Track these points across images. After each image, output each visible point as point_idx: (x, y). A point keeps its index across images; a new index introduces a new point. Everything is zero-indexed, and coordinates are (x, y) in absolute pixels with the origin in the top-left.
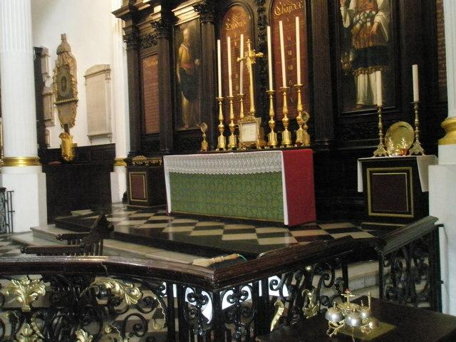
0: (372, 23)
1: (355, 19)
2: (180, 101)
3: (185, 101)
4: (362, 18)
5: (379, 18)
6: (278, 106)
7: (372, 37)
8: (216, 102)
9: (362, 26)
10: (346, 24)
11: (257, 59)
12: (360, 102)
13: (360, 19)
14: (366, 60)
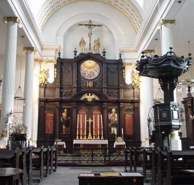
2: (62, 127)
3: (64, 127)
5: (116, 119)
6: (96, 131)
7: (115, 122)
8: (77, 128)
9: (113, 120)
10: (110, 119)
12: (112, 133)
14: (114, 125)
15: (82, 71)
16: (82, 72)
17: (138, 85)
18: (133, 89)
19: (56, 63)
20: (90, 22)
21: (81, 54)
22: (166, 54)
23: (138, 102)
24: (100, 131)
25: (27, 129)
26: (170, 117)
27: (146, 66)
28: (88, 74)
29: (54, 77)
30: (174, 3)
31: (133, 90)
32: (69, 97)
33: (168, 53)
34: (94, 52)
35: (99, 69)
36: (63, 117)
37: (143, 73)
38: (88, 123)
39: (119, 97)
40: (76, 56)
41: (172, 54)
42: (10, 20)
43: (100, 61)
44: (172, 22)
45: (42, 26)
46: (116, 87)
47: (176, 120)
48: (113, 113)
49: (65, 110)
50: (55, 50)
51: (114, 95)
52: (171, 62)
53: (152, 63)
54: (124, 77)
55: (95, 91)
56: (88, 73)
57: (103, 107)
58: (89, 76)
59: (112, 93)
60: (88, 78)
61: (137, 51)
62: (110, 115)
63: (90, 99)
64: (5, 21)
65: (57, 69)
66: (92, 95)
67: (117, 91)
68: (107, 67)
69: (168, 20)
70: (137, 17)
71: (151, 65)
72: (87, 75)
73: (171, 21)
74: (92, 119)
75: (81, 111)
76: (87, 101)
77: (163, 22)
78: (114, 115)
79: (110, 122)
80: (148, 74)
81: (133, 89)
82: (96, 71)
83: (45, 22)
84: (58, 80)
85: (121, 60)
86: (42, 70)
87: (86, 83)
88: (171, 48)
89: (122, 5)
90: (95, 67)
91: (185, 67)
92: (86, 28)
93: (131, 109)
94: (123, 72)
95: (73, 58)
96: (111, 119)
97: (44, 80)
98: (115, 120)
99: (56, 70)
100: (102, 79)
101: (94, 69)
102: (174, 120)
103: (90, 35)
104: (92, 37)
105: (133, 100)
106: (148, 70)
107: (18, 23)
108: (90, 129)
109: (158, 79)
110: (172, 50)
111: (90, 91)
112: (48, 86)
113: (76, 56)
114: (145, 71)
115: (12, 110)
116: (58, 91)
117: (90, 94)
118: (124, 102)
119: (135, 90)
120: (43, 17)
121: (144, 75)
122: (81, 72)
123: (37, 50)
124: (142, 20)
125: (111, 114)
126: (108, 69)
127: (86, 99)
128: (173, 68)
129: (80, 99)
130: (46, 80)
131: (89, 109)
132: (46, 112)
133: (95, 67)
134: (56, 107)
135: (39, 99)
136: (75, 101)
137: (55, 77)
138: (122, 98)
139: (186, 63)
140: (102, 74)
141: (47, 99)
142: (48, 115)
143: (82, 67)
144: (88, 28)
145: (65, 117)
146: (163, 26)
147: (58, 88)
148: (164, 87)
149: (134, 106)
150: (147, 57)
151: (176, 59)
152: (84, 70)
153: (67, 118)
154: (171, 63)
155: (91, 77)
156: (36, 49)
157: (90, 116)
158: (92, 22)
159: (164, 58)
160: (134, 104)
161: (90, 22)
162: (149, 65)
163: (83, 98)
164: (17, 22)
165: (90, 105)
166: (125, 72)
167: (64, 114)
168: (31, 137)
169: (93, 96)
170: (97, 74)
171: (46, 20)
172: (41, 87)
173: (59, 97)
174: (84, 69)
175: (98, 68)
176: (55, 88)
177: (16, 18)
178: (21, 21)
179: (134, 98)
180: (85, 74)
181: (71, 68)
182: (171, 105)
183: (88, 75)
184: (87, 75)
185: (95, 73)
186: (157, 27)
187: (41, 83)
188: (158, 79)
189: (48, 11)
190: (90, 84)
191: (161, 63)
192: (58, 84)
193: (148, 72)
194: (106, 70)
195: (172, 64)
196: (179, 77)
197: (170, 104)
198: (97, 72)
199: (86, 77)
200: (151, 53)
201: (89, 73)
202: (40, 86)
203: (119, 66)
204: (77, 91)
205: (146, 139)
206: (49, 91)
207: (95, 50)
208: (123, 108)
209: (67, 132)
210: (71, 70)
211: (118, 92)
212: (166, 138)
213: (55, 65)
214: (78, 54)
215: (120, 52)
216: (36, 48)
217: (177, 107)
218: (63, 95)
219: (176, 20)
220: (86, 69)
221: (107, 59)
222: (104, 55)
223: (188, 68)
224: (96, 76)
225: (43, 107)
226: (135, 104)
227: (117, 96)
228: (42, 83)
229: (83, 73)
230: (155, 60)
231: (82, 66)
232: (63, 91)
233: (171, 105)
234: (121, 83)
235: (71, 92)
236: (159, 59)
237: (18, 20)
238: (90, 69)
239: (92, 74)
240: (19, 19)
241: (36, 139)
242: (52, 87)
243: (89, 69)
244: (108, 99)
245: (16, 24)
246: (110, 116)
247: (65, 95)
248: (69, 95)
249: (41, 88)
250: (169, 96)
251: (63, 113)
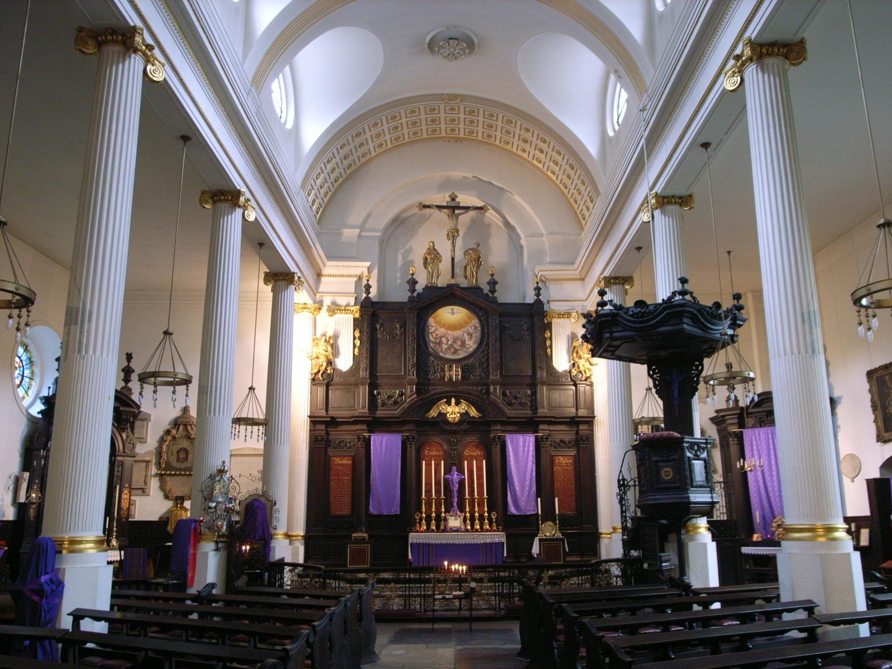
16: (432, 339)
17: (588, 375)
18: (575, 385)
19: (357, 315)
20: (453, 200)
21: (426, 288)
22: (670, 299)
23: (590, 421)
24: (481, 505)
25: (274, 508)
26: (684, 481)
27: (611, 333)
28: (447, 344)
29: (354, 354)
30: (689, 149)
31: (574, 388)
33: (674, 294)
34: (464, 283)
37: (604, 352)
39: (536, 409)
40: (415, 294)
41: (688, 297)
42: (220, 200)
43: (481, 309)
44: (684, 201)
45: (317, 212)
46: (528, 381)
47: (701, 486)
50: (355, 279)
51: (521, 404)
52: (685, 320)
53: (630, 324)
54: (549, 350)
55: (470, 394)
56: (448, 340)
57: (492, 436)
58: (452, 350)
59: (516, 398)
60: (447, 356)
61: (583, 279)
63: (453, 416)
64: (207, 202)
67: (529, 392)
68: (500, 322)
69: (673, 196)
70: (583, 183)
71: (629, 330)
72: (444, 346)
73: (680, 198)
75: (429, 450)
77: (657, 201)
80: (617, 353)
81: (575, 385)
82: (470, 335)
83: (326, 200)
84: (365, 363)
85: (539, 303)
86: (318, 335)
87: (443, 370)
88: (683, 281)
89: (542, 151)
90: (466, 323)
91: (726, 334)
92: (443, 215)
93: (570, 442)
94: (545, 339)
95: (406, 300)
97: (325, 364)
99: (357, 334)
100: (488, 358)
101: (465, 329)
102: (696, 487)
103: (453, 235)
104: (459, 242)
106: (618, 343)
107: (245, 208)
108: (454, 498)
109: (645, 367)
110: (686, 285)
111: (455, 394)
112: (336, 379)
113: (415, 294)
114: (609, 346)
115: (224, 462)
116: (363, 392)
117: (453, 400)
118: (550, 423)
119: (581, 388)
120: (321, 187)
121: (604, 354)
123: (302, 279)
124: (598, 193)
126: (502, 329)
127: (442, 415)
128: (692, 337)
130: (330, 363)
131: (450, 443)
132: (331, 452)
133: (466, 323)
134: (359, 439)
135: (310, 417)
136: (409, 422)
137: (356, 354)
138: (542, 412)
139: (728, 322)
141: (332, 418)
142: (338, 460)
144: (446, 217)
146: (657, 213)
147: (363, 384)
148: (663, 389)
149: (577, 433)
150: (615, 306)
151: (699, 311)
154: (683, 323)
155: (456, 352)
156: (299, 278)
157: (454, 462)
158: (457, 200)
159: (665, 309)
161: (453, 200)
162: (620, 329)
163: (433, 413)
164: (239, 207)
165: (455, 432)
168: (288, 529)
169: (464, 407)
170: (474, 342)
171: (330, 194)
172: (316, 382)
173: (366, 410)
175: (476, 328)
176: (356, 385)
177: (238, 193)
178: (253, 202)
179: (577, 410)
180: (440, 343)
181: (401, 327)
182: (685, 445)
183: (449, 348)
184: (444, 346)
185: (467, 342)
186: (641, 214)
187: (316, 371)
188: (645, 367)
189: (334, 169)
190: (455, 373)
191: (654, 324)
192: (364, 374)
193: (617, 347)
195: (687, 327)
196: (706, 361)
197: (683, 442)
199: (441, 354)
200: (623, 284)
201: (450, 343)
202: (313, 380)
203: (534, 319)
204: (418, 392)
205: (614, 529)
206: (337, 392)
207: (466, 277)
208: (547, 438)
210: (401, 334)
211: (534, 394)
212: (673, 537)
213: (355, 319)
214: (419, 288)
215: (537, 283)
216: (299, 274)
217: (704, 450)
218: (380, 405)
219: (695, 197)
220: (442, 331)
221: (499, 301)
222: (493, 291)
223: (732, 336)
224: (471, 349)
225: (322, 439)
226: (582, 427)
227: (529, 404)
228: (319, 371)
230: (637, 314)
231: (431, 321)
232: (379, 393)
233: (685, 445)
234: (540, 368)
235: (401, 395)
236: (650, 313)
237: (242, 199)
238: (453, 327)
239: (459, 343)
240: (248, 195)
241: (300, 530)
242: (349, 380)
244: (503, 413)
245: (239, 212)
247: (383, 404)
248: (396, 403)
249: (315, 385)
250: (678, 413)
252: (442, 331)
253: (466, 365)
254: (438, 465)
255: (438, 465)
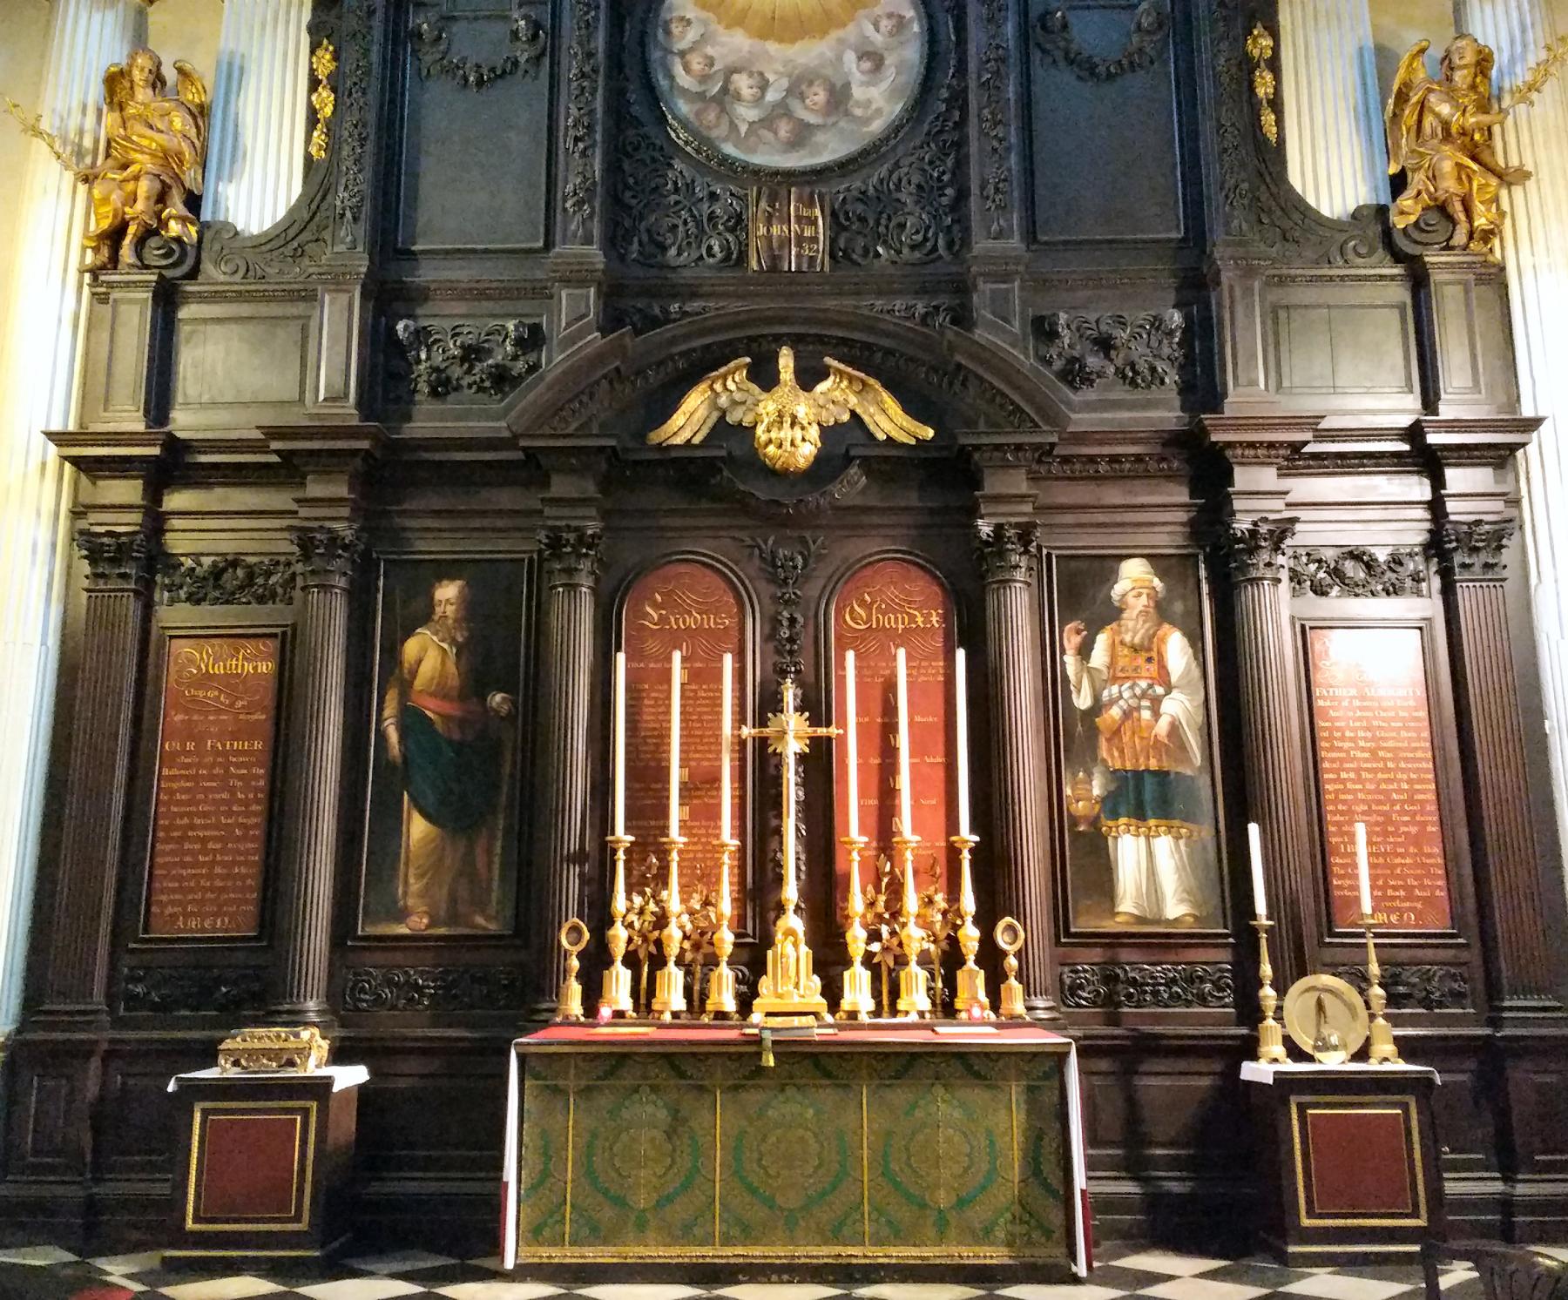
0: (1157, 714)
1: (1105, 693)
3: (418, 828)
4: (1126, 695)
9: (1127, 715)
10: (1083, 701)
11: (815, 742)
13: (1121, 697)
14: (1146, 796)
15: (678, 69)
16: (684, 80)
17: (1480, 222)
28: (758, 100)
29: (308, 159)
32: (504, 414)
35: (916, 28)
36: (406, 687)
38: (762, 768)
48: (1134, 625)
49: (448, 593)
54: (1268, 118)
56: (764, 86)
58: (784, 129)
59: (1105, 345)
60: (758, 159)
62: (1085, 651)
65: (336, 57)
66: (823, 374)
74: (817, 707)
75: (669, 604)
76: (753, 464)
78: (1149, 650)
79: (1094, 748)
82: (874, 59)
87: (738, 222)
93: (1396, 561)
94: (1248, 66)
96: (1097, 708)
98: (1162, 727)
99: (325, 64)
101: (850, 32)
105: (1405, 421)
117: (786, 362)
122: (663, 83)
125: (1102, 640)
127: (730, 434)
129: (656, 437)
131: (776, 573)
132: (172, 614)
134: (306, 543)
140: (959, 99)
143: (689, 22)
145: (440, 692)
149: (1436, 506)
152: (710, 51)
153: (463, 696)
155: (802, 135)
160: (1438, 483)
163: (689, 420)
166: (1274, 65)
167: (428, 654)
169: (837, 395)
170: (893, 93)
173: (348, 412)
174: (704, 39)
175: (901, 24)
180: (725, 97)
181: (536, 26)
183: (767, 122)
184: (747, 114)
185: (858, 92)
190: (797, 236)
192: (347, 248)
194: (1010, 29)
198: (890, 72)
199: (729, 149)
201: (772, 96)
204: (611, 320)
209: (463, 893)
210: (537, 60)
220: (734, 43)
224: (877, 126)
226: (1457, 478)
227: (1172, 378)
229: (701, 96)
239: (819, 96)
243: (772, 47)
246: (1092, 668)
251: (409, 633)
252: (734, 43)
253: (854, 197)
254: (703, 677)
255: (703, 677)
